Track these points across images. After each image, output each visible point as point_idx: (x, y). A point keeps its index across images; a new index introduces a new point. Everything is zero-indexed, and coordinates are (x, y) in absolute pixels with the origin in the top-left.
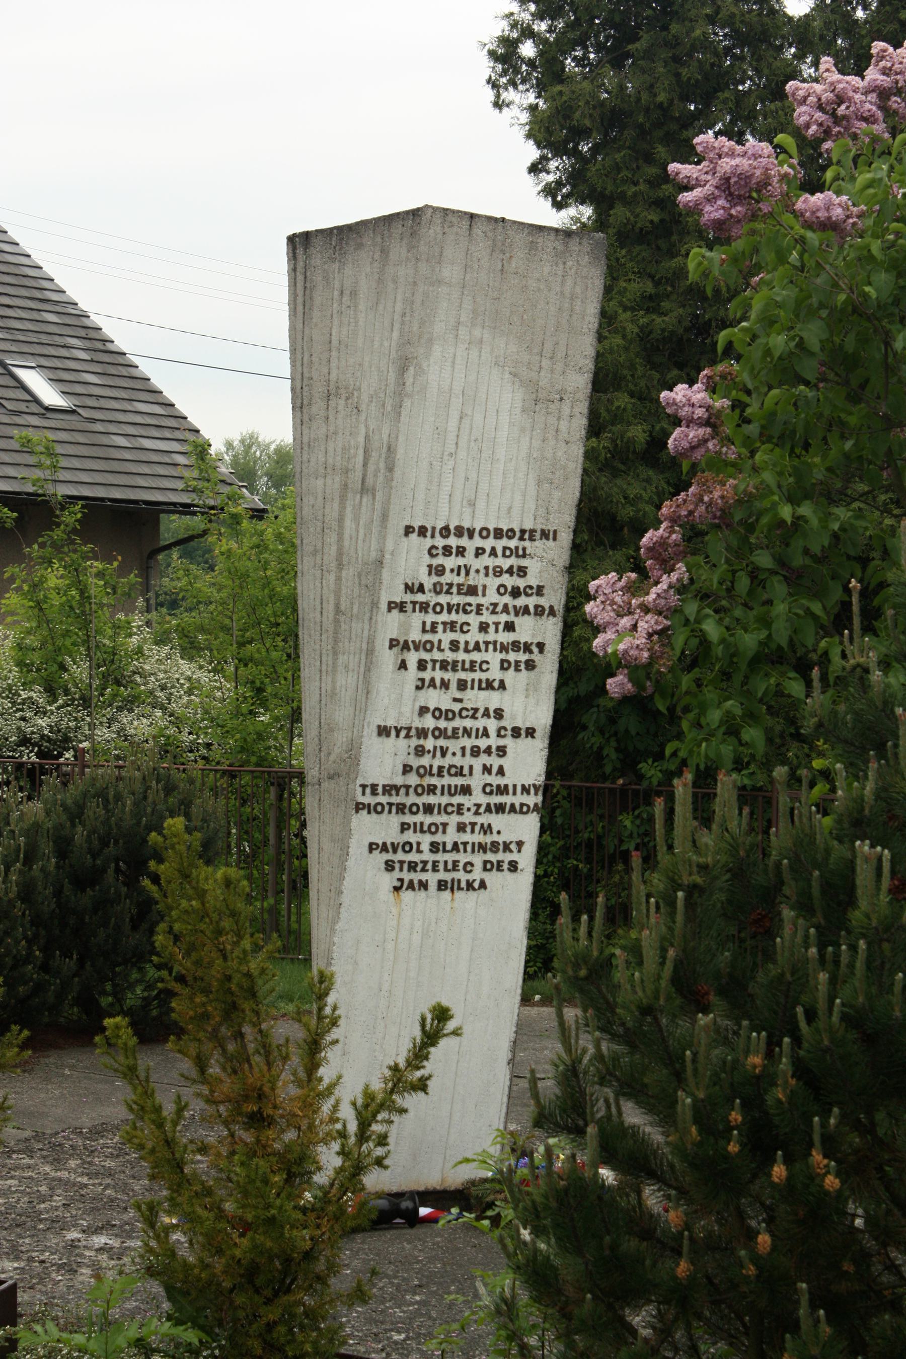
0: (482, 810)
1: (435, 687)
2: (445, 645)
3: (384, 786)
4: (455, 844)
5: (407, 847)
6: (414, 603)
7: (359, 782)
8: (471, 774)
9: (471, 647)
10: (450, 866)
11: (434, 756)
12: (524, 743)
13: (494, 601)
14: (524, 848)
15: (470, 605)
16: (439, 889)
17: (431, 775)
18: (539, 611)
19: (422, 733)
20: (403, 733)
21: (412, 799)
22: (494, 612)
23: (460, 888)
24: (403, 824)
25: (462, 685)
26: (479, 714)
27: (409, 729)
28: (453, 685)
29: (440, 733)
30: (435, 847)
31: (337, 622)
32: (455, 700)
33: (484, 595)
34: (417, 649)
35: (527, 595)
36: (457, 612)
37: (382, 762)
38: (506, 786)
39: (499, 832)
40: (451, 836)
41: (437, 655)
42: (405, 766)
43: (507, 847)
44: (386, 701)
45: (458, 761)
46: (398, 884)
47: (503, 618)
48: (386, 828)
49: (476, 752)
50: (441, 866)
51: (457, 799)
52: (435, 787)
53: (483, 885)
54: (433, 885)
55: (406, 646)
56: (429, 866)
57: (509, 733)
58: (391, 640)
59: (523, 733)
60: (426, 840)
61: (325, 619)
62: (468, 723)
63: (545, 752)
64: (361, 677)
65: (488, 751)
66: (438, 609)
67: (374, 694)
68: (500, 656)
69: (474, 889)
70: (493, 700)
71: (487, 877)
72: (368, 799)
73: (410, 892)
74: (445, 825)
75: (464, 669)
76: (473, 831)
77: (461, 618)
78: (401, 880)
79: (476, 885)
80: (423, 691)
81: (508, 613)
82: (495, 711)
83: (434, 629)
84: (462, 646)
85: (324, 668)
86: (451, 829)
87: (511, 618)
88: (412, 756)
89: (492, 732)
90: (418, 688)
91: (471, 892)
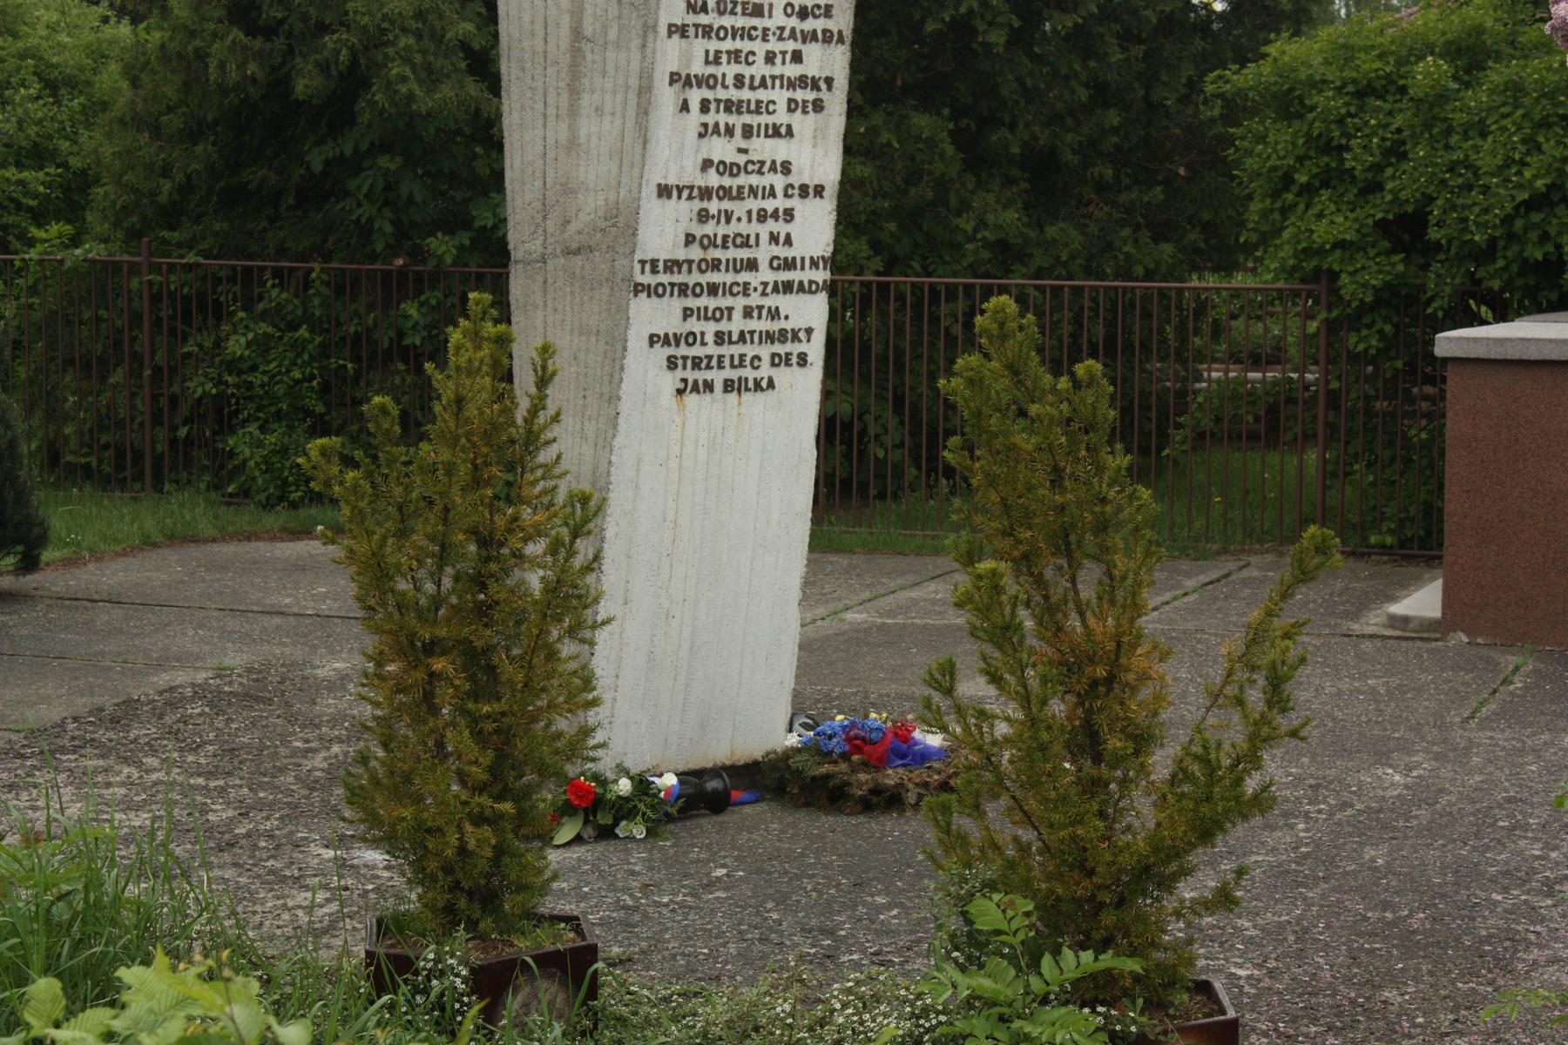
0: (769, 289)
1: (719, 134)
2: (730, 81)
3: (665, 262)
4: (742, 333)
5: (691, 338)
6: (696, 26)
7: (637, 257)
8: (757, 244)
9: (757, 83)
10: (736, 362)
11: (718, 222)
12: (813, 203)
13: (781, 24)
14: (813, 336)
15: (755, 28)
16: (726, 391)
17: (716, 246)
18: (828, 37)
19: (706, 193)
20: (685, 194)
21: (695, 278)
22: (781, 39)
23: (747, 389)
24: (685, 309)
25: (748, 132)
26: (765, 169)
27: (691, 188)
28: (738, 132)
29: (725, 193)
30: (720, 338)
31: (576, 52)
32: (741, 151)
33: (770, 16)
34: (699, 86)
35: (815, 17)
36: (742, 38)
37: (663, 230)
38: (794, 259)
39: (787, 317)
40: (737, 324)
41: (721, 94)
42: (687, 235)
43: (795, 337)
44: (666, 153)
45: (743, 228)
46: (681, 386)
47: (790, 46)
48: (660, 315)
49: (762, 216)
50: (727, 362)
51: (744, 277)
52: (719, 261)
53: (771, 384)
54: (719, 386)
55: (688, 83)
56: (714, 363)
57: (796, 192)
58: (672, 74)
59: (811, 191)
60: (710, 328)
61: (551, 47)
62: (754, 180)
63: (834, 216)
64: (630, 123)
65: (775, 215)
66: (722, 33)
67: (651, 146)
68: (787, 94)
69: (762, 390)
70: (776, 150)
71: (774, 372)
72: (647, 279)
73: (694, 395)
74: (730, 309)
75: (749, 112)
76: (760, 317)
77: (745, 45)
78: (685, 381)
79: (764, 384)
80: (706, 139)
81: (796, 40)
82: (783, 164)
83: (717, 61)
84: (747, 81)
85: (551, 111)
86: (737, 315)
87: (798, 46)
88: (694, 223)
89: (779, 191)
90: (701, 136)
91: (759, 393)
